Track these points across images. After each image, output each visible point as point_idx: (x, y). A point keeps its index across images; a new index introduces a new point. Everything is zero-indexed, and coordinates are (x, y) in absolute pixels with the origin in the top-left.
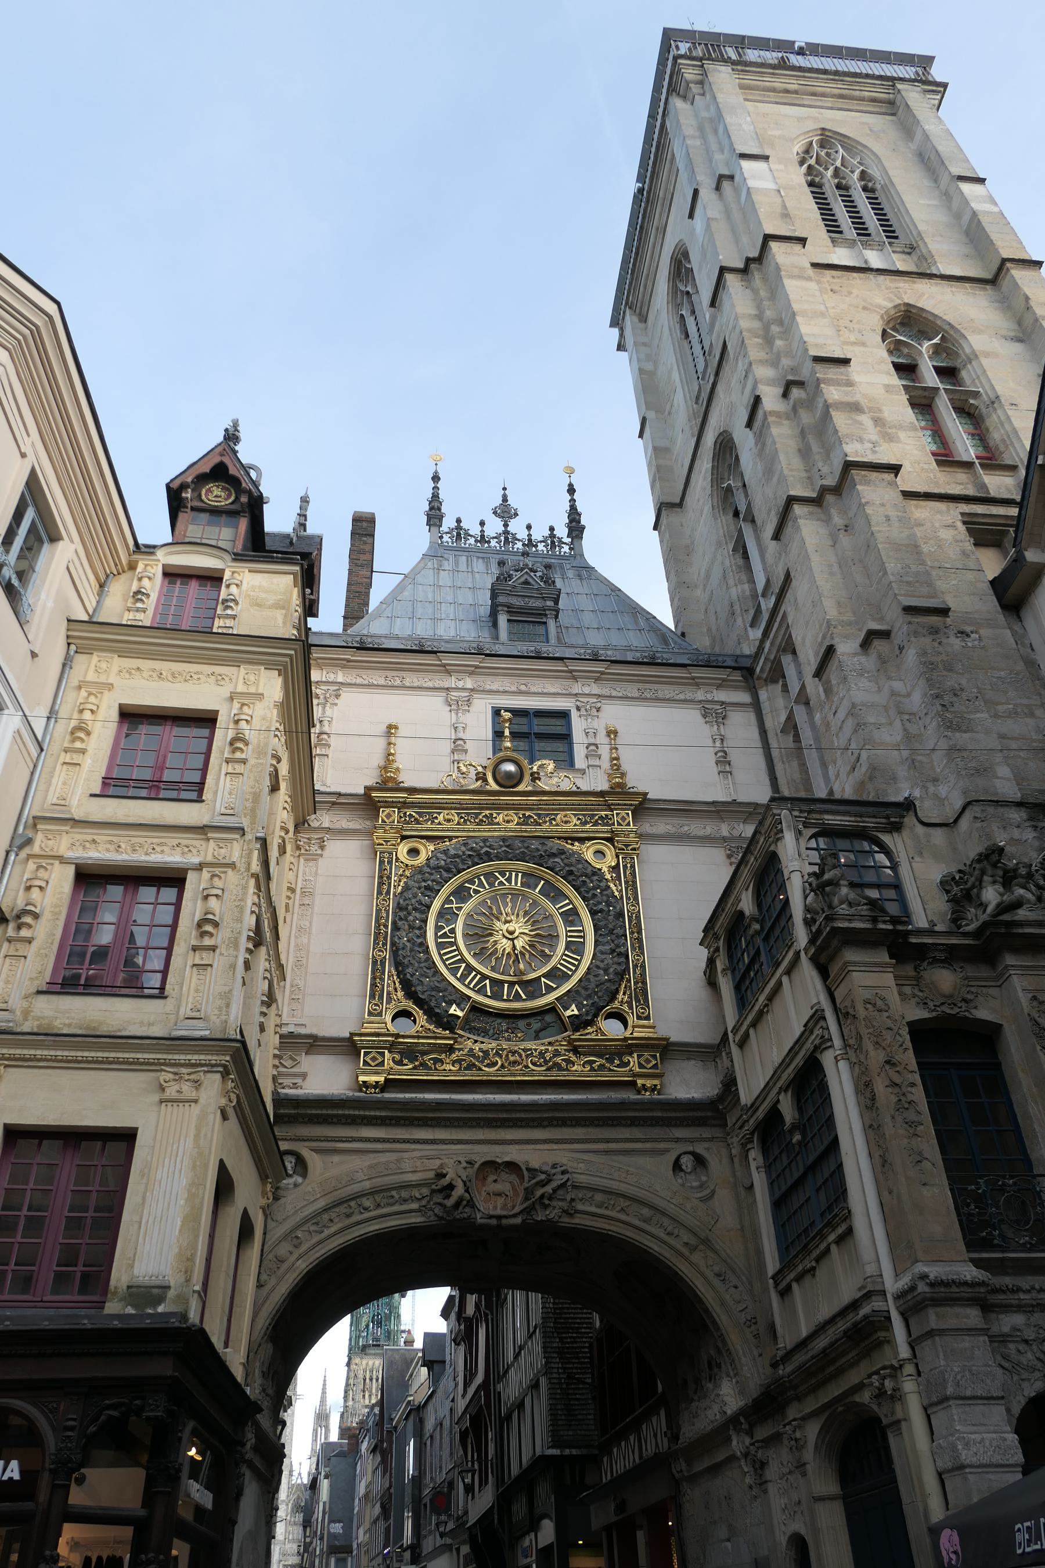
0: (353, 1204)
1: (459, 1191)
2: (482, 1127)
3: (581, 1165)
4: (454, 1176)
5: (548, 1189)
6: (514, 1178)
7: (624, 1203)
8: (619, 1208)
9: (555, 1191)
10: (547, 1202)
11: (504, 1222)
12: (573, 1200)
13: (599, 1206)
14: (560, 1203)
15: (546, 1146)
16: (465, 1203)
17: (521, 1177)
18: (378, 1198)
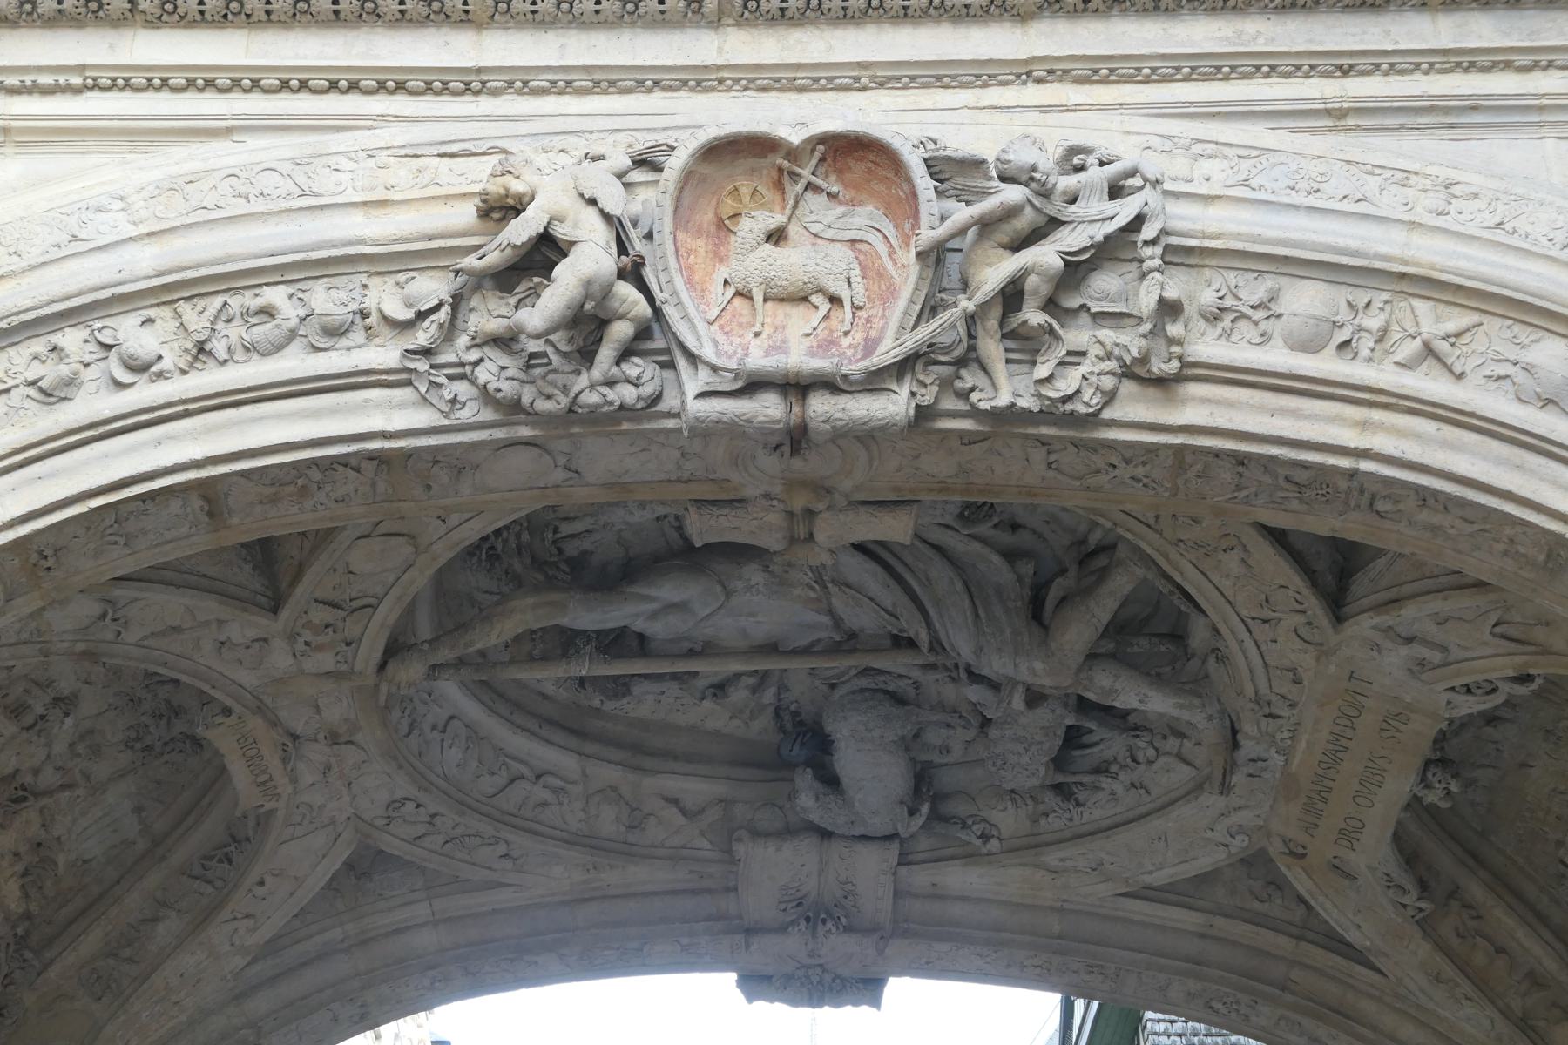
0: (72, 339)
1: (590, 258)
2: (716, 23)
3: (1206, 166)
4: (568, 203)
5: (1046, 256)
6: (866, 218)
7: (1432, 319)
8: (1412, 347)
9: (1076, 270)
10: (1033, 316)
11: (821, 406)
12: (1169, 309)
13: (1309, 346)
14: (1108, 335)
15: (1033, 94)
16: (621, 331)
17: (906, 208)
18: (196, 317)
